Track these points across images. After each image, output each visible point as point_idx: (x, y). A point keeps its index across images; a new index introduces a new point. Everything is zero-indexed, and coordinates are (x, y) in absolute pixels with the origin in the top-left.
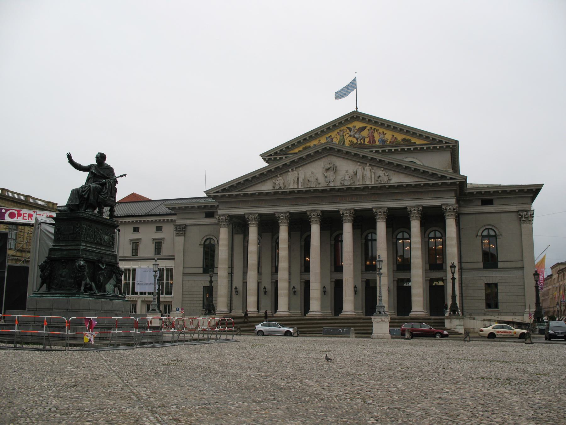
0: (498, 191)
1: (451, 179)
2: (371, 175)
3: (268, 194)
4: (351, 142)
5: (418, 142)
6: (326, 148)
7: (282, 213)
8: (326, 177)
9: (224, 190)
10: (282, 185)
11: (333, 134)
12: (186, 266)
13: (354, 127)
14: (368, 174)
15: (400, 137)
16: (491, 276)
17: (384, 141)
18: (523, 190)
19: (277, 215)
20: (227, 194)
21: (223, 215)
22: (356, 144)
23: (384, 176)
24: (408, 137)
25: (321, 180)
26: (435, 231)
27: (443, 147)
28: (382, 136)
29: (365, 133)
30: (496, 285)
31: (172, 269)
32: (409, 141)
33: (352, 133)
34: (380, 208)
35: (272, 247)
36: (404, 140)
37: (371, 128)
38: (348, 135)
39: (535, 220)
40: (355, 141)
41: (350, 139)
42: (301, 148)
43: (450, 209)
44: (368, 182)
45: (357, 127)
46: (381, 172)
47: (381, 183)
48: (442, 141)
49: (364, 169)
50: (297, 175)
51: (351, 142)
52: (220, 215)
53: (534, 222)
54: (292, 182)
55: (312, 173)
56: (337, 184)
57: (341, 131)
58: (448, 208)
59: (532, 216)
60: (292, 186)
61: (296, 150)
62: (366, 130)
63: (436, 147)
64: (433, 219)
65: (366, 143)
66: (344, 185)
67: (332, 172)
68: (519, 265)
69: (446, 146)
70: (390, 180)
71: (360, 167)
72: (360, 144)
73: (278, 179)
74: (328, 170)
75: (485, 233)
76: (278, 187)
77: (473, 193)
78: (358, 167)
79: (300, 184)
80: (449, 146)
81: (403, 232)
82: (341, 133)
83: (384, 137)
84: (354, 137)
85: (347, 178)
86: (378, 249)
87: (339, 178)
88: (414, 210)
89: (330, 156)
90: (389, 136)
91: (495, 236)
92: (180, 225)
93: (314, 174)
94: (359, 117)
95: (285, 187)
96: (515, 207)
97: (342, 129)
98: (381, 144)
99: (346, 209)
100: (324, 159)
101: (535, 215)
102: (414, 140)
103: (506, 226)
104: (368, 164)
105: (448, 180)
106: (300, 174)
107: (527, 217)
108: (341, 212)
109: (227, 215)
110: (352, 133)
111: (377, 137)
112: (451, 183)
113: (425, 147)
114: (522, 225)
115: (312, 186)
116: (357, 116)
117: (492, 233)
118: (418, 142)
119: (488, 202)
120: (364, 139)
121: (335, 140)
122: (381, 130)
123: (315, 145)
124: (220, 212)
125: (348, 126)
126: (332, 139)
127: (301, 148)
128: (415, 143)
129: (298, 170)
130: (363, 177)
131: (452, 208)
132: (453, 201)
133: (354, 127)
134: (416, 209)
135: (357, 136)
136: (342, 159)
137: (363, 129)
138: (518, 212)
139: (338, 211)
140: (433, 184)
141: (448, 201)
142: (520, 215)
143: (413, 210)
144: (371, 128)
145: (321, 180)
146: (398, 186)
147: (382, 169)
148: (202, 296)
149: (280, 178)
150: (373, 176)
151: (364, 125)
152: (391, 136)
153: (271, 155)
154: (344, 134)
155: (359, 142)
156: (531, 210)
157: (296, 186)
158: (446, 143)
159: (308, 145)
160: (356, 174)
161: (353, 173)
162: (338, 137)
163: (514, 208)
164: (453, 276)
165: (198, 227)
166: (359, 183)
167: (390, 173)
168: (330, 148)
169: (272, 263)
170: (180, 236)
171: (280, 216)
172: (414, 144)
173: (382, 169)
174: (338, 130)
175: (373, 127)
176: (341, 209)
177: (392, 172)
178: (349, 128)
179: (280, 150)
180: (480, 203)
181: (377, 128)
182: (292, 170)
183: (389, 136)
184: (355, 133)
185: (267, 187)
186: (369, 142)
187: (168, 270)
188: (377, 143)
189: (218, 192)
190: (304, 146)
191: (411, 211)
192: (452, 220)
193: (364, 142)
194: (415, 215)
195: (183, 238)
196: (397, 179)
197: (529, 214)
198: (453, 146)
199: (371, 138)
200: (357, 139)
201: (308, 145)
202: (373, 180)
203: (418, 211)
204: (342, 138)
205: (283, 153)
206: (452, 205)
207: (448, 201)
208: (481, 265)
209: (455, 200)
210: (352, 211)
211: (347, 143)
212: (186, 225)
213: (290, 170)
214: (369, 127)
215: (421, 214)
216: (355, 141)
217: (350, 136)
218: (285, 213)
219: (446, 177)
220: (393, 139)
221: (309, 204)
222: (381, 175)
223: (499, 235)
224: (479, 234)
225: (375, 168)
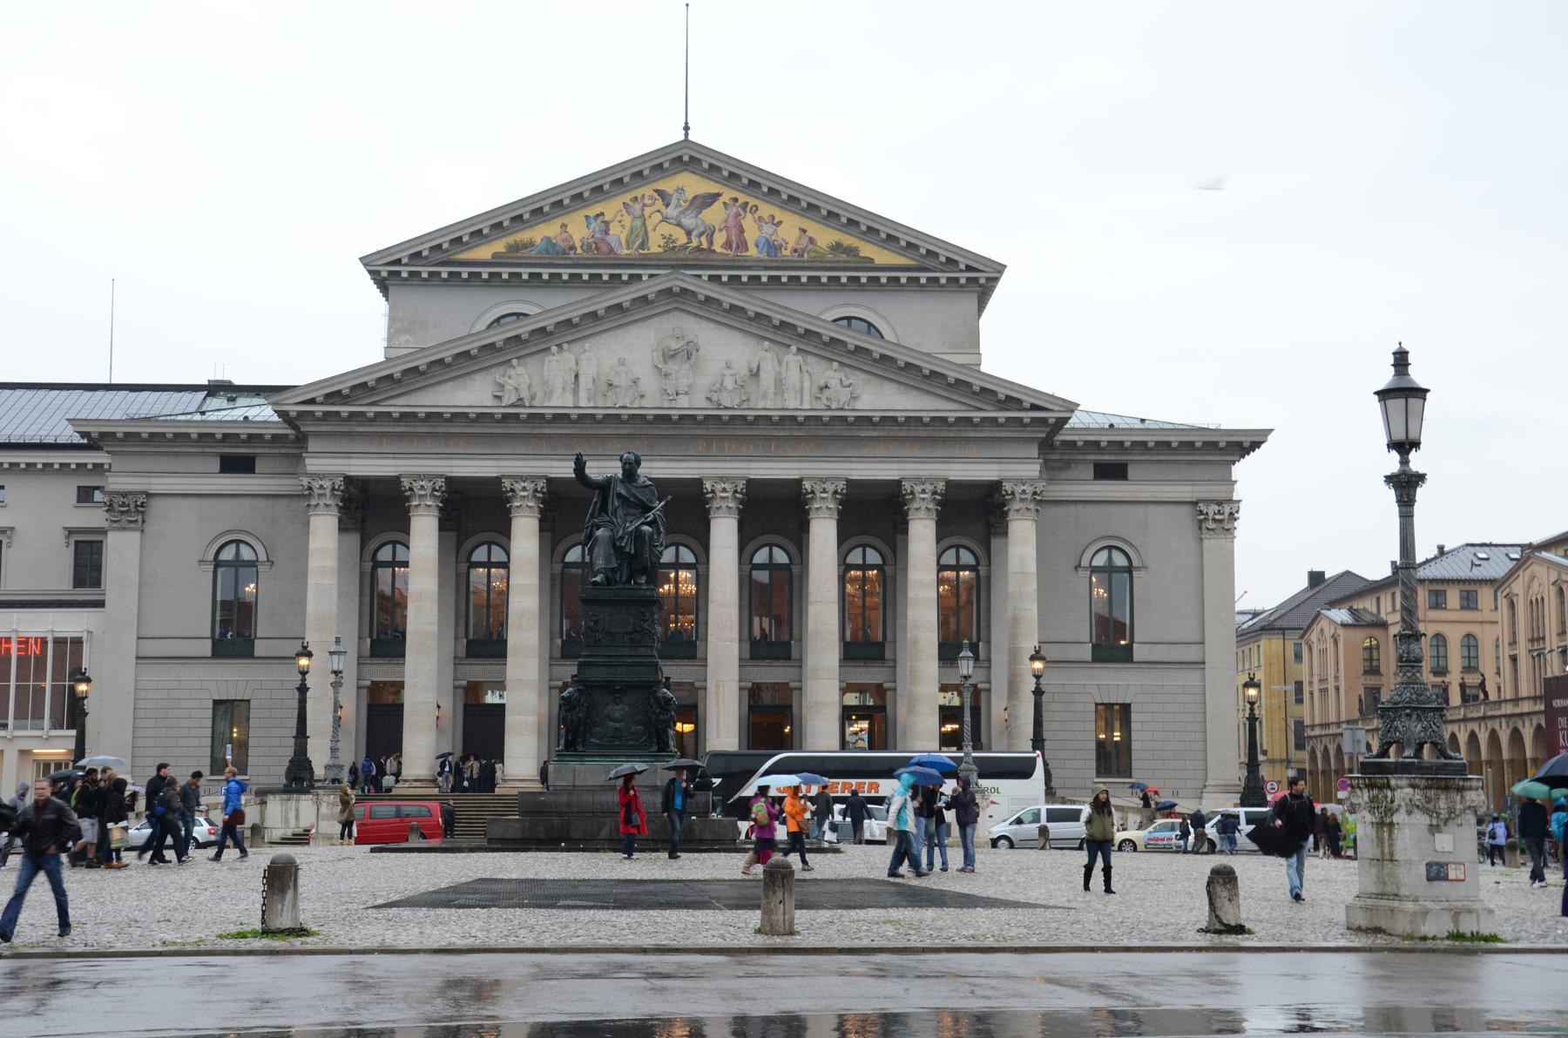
0: (1144, 443)
1: (1034, 407)
2: (802, 381)
3: (481, 417)
4: (669, 239)
5: (882, 257)
6: (669, 290)
7: (523, 478)
8: (666, 375)
9: (335, 397)
10: (525, 394)
11: (611, 208)
12: (145, 632)
13: (681, 190)
14: (793, 376)
15: (825, 237)
16: (1115, 683)
17: (773, 247)
18: (1215, 444)
19: (507, 484)
20: (345, 410)
21: (322, 476)
22: (684, 247)
23: (839, 388)
24: (849, 240)
25: (650, 384)
26: (958, 547)
27: (957, 279)
29: (714, 215)
30: (1126, 709)
31: (77, 642)
32: (851, 251)
34: (823, 480)
35: (458, 575)
36: (837, 247)
37: (736, 200)
38: (658, 217)
39: (1244, 527)
40: (682, 239)
41: (666, 229)
42: (499, 246)
43: (1024, 492)
44: (792, 403)
45: (689, 195)
46: (830, 373)
47: (829, 408)
48: (956, 263)
49: (780, 363)
50: (573, 364)
51: (669, 239)
52: (315, 476)
53: (1236, 533)
54: (559, 386)
55: (622, 362)
56: (693, 402)
58: (1019, 489)
59: (1233, 517)
60: (560, 400)
61: (484, 252)
62: (718, 204)
63: (937, 280)
64: (975, 515)
65: (717, 247)
67: (687, 366)
68: (1192, 654)
69: (968, 279)
70: (854, 398)
71: (769, 355)
72: (698, 249)
73: (512, 372)
74: (670, 356)
75: (1101, 560)
76: (513, 399)
77: (1074, 442)
78: (763, 354)
79: (583, 394)
80: (976, 280)
81: (864, 546)
82: (638, 207)
84: (679, 225)
85: (729, 383)
86: (812, 598)
87: (704, 382)
88: (924, 491)
90: (790, 229)
91: (1129, 570)
92: (124, 495)
93: (624, 367)
94: (699, 161)
95: (533, 398)
96: (1189, 488)
97: (638, 193)
98: (764, 256)
99: (723, 479)
100: (655, 323)
101: (1240, 515)
102: (867, 250)
103: (1161, 542)
104: (794, 348)
105: (1025, 410)
107: (1221, 521)
108: (708, 485)
109: (338, 475)
110: (671, 211)
111: (752, 233)
112: (1034, 420)
113: (903, 277)
114: (1206, 542)
115: (623, 401)
117: (1119, 560)
118: (882, 257)
119: (1112, 471)
120: (710, 234)
121: (614, 229)
122: (766, 210)
123: (548, 239)
124: (313, 464)
125: (661, 186)
126: (607, 223)
127: (499, 246)
128: (872, 260)
129: (577, 347)
130: (779, 384)
131: (1029, 490)
132: (1033, 470)
133: (681, 190)
134: (929, 488)
135: (688, 221)
136: (712, 325)
137: (709, 200)
138: (1195, 503)
139: (698, 482)
140: (983, 419)
141: (1016, 469)
142: (1201, 513)
143: (918, 489)
144: (736, 200)
145: (650, 384)
146: (883, 419)
147: (835, 365)
148: (209, 732)
149: (520, 370)
150: (807, 385)
151: (713, 188)
152: (797, 232)
153: (398, 262)
154: (647, 211)
155: (695, 243)
156: (1230, 501)
157: (568, 401)
158: (969, 268)
159: (524, 236)
160: (755, 374)
161: (745, 372)
162: (627, 220)
163: (1185, 492)
164: (1038, 684)
165: (195, 502)
166: (765, 402)
167: (857, 378)
168: (683, 290)
169: (457, 625)
170: (124, 529)
171: (518, 487)
172: (868, 264)
173: (835, 365)
174: (627, 198)
175: (742, 198)
176: (709, 478)
177: (863, 376)
178: (660, 193)
179: (432, 249)
180: (1091, 474)
181: (752, 201)
182: (559, 346)
183: (790, 229)
185: (473, 394)
186: (728, 245)
187: (59, 642)
188: (753, 252)
189: (312, 401)
190: (511, 239)
191: (912, 493)
192: (1029, 523)
193: (711, 243)
194: (924, 505)
195: (137, 535)
196: (879, 398)
197: (1227, 510)
198: (988, 279)
199: (734, 232)
200: (689, 233)
201: (524, 236)
202: (807, 397)
203: (935, 493)
204: (638, 223)
205: (439, 257)
206: (1031, 481)
207: (1016, 469)
208: (1086, 652)
209: (1038, 467)
210: (741, 485)
211: (655, 246)
212: (149, 495)
213: (554, 349)
214: (727, 194)
215: (939, 503)
216: (682, 239)
217: (665, 219)
218: (533, 478)
219: (1019, 401)
220: (805, 241)
222: (834, 383)
223: (1139, 568)
224: (1085, 563)
225: (811, 359)
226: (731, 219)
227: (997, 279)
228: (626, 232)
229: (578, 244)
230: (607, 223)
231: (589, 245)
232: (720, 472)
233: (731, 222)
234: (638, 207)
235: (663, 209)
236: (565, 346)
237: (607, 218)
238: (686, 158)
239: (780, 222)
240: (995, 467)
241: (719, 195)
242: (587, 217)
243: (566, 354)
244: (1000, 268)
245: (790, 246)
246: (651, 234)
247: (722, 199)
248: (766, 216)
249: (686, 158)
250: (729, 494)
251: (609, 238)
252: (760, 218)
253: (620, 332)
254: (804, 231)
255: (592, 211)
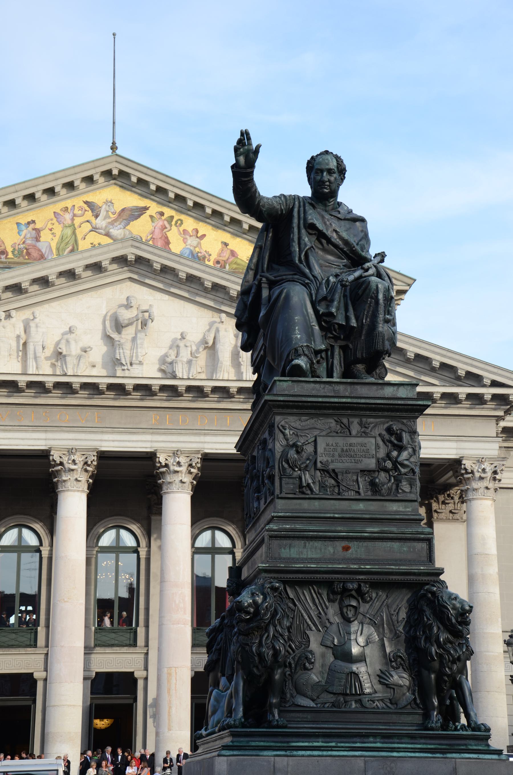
1: (495, 384)
13: (109, 203)
28: (192, 241)
29: (142, 227)
33: (100, 222)
37: (162, 214)
38: (87, 227)
50: (20, 329)
57: (66, 209)
62: (145, 217)
66: (174, 377)
82: (68, 217)
83: (199, 244)
84: (108, 235)
89: (129, 283)
97: (69, 203)
100: (108, 291)
105: (484, 386)
106: (33, 330)
110: (100, 222)
111: (177, 246)
112: (495, 397)
116: (121, 172)
121: (45, 236)
126: (38, 231)
131: (489, 469)
135: (117, 232)
152: (220, 246)
154: (77, 221)
162: (58, 229)
174: (58, 207)
175: (168, 212)
184: (112, 223)
204: (69, 231)
214: (154, 208)
217: (94, 229)
220: (226, 254)
221: (59, 428)
226: (157, 231)
227: (404, 292)
228: (56, 239)
229: (9, 250)
230: (38, 231)
231: (20, 251)
232: (175, 446)
233: (157, 234)
234: (68, 217)
235: (93, 219)
236: (13, 313)
237: (38, 226)
238: (115, 172)
239: (204, 236)
240: (453, 445)
241: (146, 209)
242: (18, 224)
243: (13, 320)
244: (411, 281)
245: (213, 258)
246: (81, 243)
247: (148, 213)
248: (190, 229)
249: (115, 172)
250: (184, 469)
251: (39, 245)
252: (184, 231)
253: (71, 301)
254: (226, 244)
255: (23, 219)
